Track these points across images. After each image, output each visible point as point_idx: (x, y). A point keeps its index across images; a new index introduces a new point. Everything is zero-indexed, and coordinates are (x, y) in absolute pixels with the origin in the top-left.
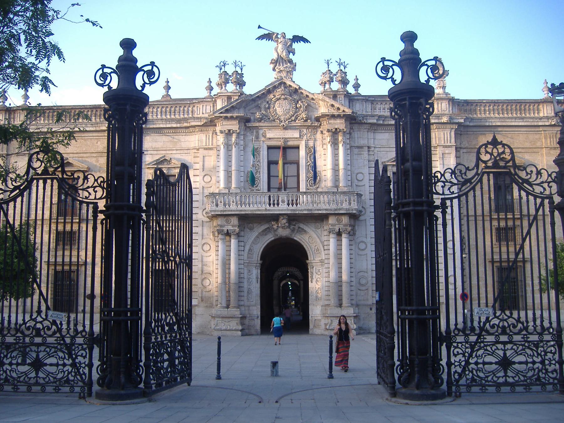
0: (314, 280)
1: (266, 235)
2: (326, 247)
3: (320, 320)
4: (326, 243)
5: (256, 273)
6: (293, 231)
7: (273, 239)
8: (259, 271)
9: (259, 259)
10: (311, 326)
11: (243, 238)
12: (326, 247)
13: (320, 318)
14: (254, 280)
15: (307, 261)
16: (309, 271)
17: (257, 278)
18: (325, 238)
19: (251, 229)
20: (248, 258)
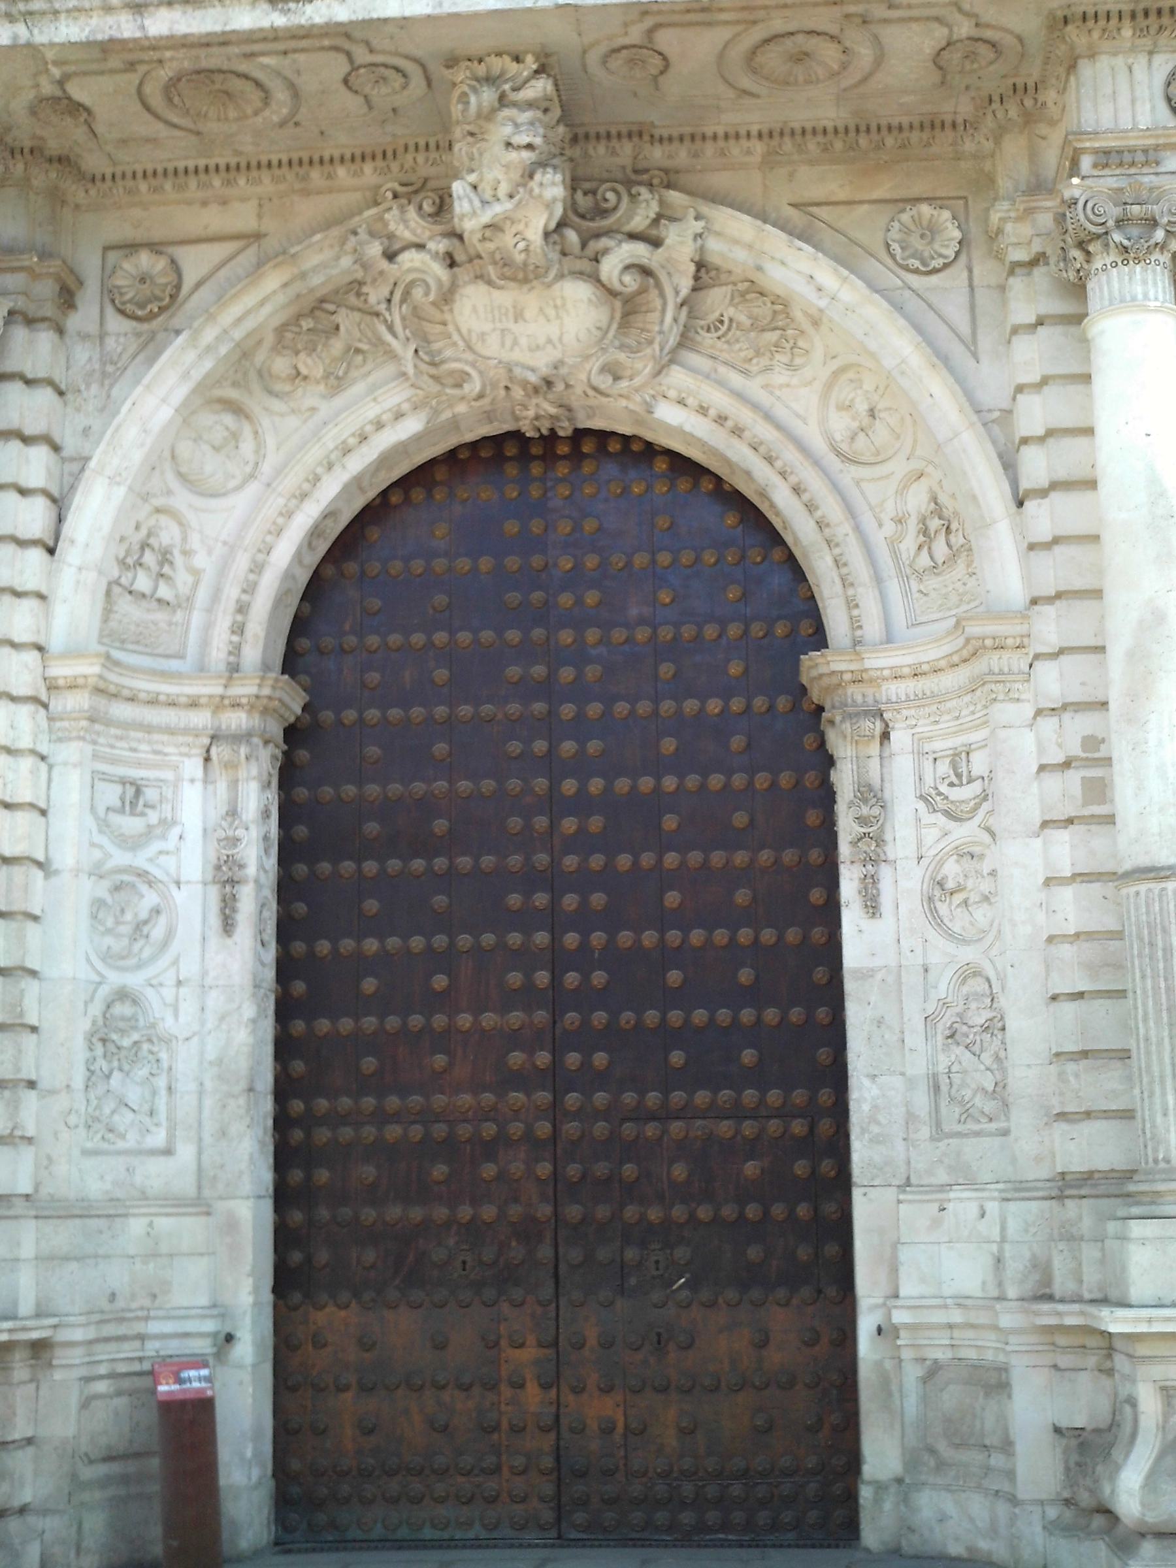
0: (902, 883)
1: (336, 383)
2: (1036, 466)
3: (994, 1382)
4: (1033, 415)
5: (211, 819)
6: (627, 309)
7: (412, 426)
8: (256, 798)
9: (252, 655)
10: (881, 1453)
11: (45, 396)
12: (1036, 466)
13: (982, 1348)
14: (192, 904)
15: (817, 666)
16: (844, 780)
17: (226, 876)
18: (1032, 356)
19: (155, 310)
20: (112, 635)
